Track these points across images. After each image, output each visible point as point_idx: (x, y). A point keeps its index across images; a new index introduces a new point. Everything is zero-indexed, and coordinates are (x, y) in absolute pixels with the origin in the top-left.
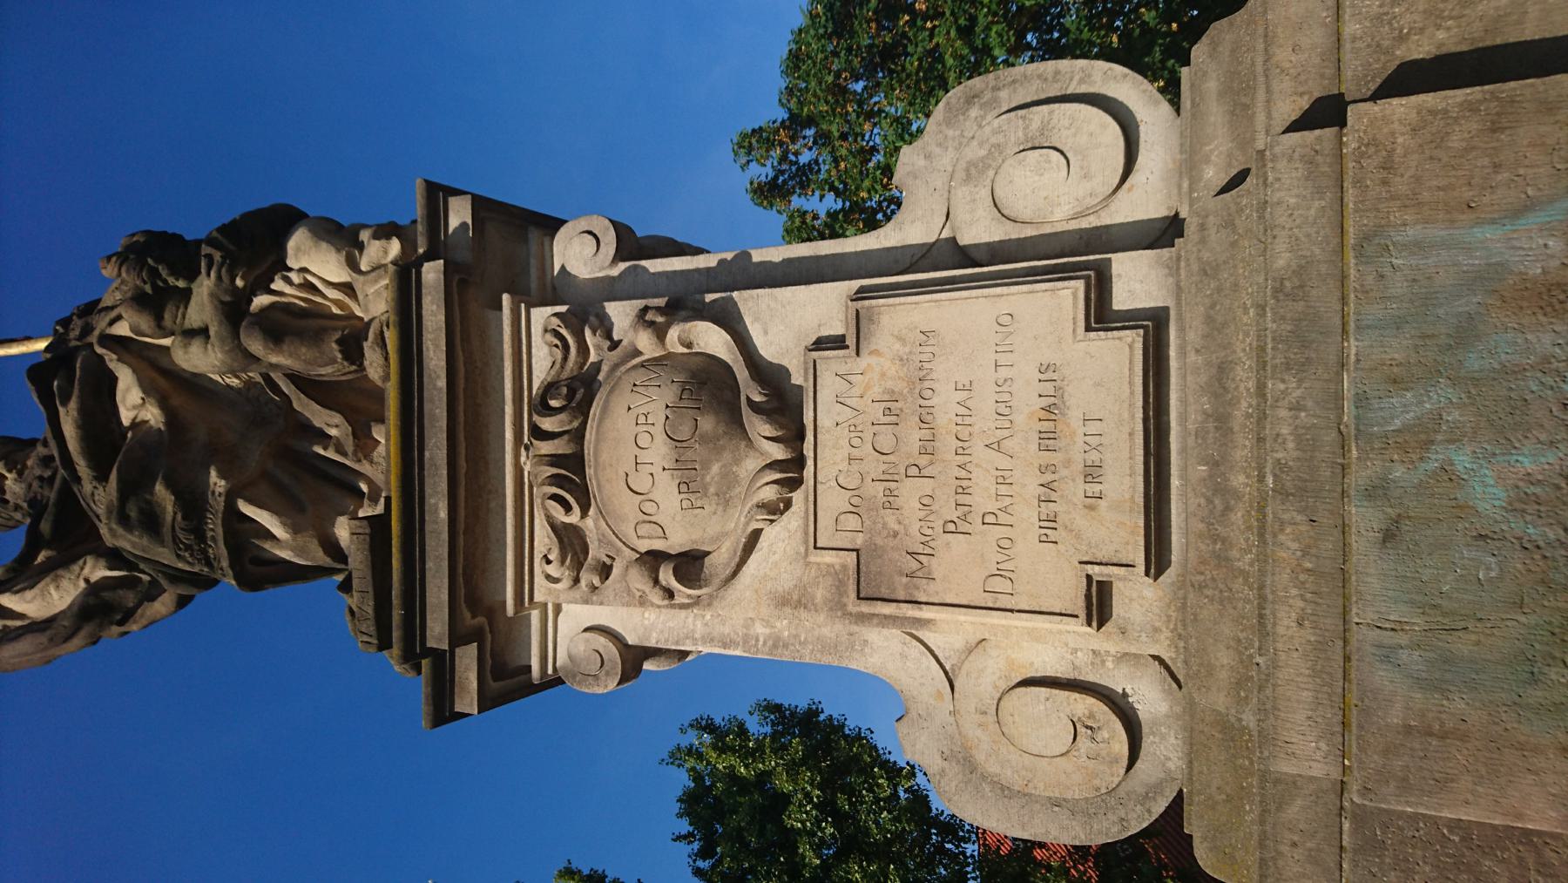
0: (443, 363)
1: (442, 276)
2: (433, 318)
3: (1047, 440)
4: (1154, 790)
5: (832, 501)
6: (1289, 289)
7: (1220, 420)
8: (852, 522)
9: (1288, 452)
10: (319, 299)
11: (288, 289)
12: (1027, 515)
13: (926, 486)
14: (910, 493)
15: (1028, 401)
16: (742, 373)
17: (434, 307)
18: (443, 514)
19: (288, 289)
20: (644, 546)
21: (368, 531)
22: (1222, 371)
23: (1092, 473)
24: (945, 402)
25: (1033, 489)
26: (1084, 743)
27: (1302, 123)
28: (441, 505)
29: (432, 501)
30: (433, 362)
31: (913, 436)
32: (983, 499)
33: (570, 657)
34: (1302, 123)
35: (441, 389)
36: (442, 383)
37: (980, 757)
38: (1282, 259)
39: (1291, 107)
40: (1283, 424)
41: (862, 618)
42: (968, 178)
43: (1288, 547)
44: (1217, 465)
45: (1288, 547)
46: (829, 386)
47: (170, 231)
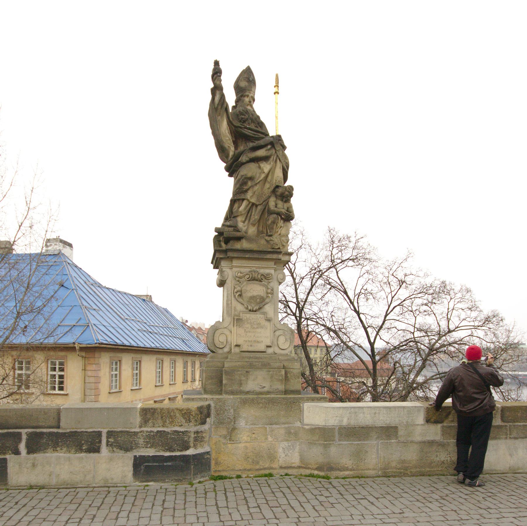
3: (255, 341)
4: (216, 350)
5: (248, 316)
6: (269, 364)
7: (257, 358)
8: (245, 318)
9: (254, 364)
12: (247, 339)
13: (250, 328)
14: (248, 326)
15: (259, 339)
16: (263, 303)
18: (247, 256)
20: (243, 289)
22: (261, 358)
23: (251, 346)
24: (259, 330)
25: (249, 340)
26: (220, 343)
27: (284, 366)
31: (255, 326)
32: (248, 334)
33: (224, 271)
34: (284, 366)
37: (217, 331)
38: (272, 364)
39: (285, 364)
40: (257, 363)
41: (234, 319)
42: (283, 332)
43: (245, 364)
44: (252, 358)
45: (245, 364)
46: (262, 316)
47: (294, 192)
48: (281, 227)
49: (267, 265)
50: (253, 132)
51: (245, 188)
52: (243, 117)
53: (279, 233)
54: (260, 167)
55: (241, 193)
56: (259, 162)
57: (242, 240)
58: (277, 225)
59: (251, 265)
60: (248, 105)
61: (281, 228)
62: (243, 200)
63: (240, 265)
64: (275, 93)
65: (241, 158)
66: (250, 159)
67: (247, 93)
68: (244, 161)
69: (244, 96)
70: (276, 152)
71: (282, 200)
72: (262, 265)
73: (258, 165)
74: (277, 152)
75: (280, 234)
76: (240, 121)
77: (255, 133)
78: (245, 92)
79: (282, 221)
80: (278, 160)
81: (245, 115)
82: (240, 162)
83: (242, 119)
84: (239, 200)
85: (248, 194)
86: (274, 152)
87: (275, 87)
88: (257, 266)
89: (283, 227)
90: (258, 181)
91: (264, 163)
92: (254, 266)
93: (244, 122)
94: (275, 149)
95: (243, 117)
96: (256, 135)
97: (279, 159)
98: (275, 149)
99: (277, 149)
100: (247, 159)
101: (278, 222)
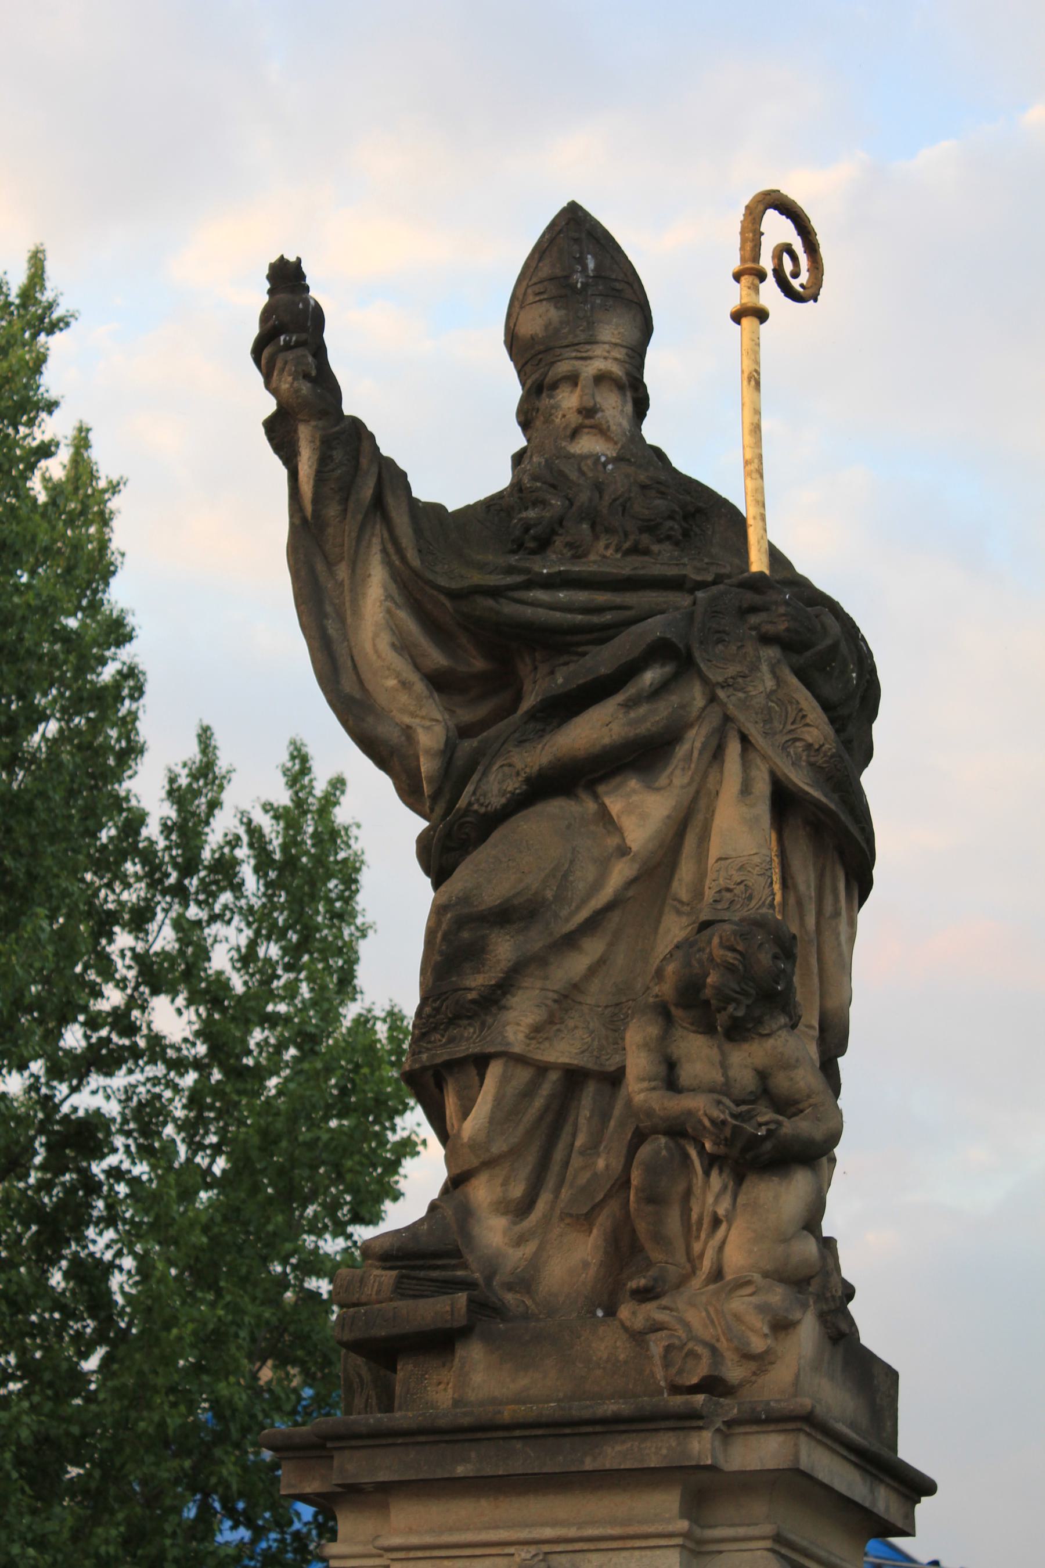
0: (608, 1466)
1: (694, 1463)
2: (653, 1450)
10: (703, 1235)
11: (710, 1200)
17: (664, 1451)
18: (460, 1470)
19: (710, 1200)
21: (456, 1325)
28: (470, 1467)
29: (473, 1455)
30: (609, 1450)
35: (583, 1462)
36: (589, 1465)
48: (716, 1222)
49: (555, 1524)
50: (582, 597)
51: (477, 981)
52: (531, 514)
53: (707, 1264)
54: (605, 816)
55: (454, 1020)
56: (601, 789)
57: (460, 1352)
58: (686, 1211)
59: (503, 1535)
60: (575, 434)
61: (723, 1227)
62: (481, 1062)
63: (429, 1539)
64: (737, 317)
65: (469, 788)
66: (528, 780)
67: (563, 368)
68: (497, 801)
69: (554, 386)
70: (713, 699)
71: (708, 1029)
72: (580, 1525)
73: (591, 806)
74: (721, 694)
75: (717, 1275)
76: (519, 546)
77: (601, 598)
78: (552, 364)
79: (716, 1181)
80: (733, 749)
81: (543, 503)
82: (467, 811)
83: (527, 529)
84: (454, 1065)
85: (511, 1015)
86: (699, 701)
87: (737, 277)
88: (548, 1533)
89: (730, 1218)
90: (584, 914)
91: (633, 783)
92: (524, 1534)
93: (543, 544)
94: (705, 680)
95: (531, 514)
96: (600, 610)
97: (745, 740)
98: (705, 680)
99: (715, 676)
100: (514, 785)
101: (688, 1194)
